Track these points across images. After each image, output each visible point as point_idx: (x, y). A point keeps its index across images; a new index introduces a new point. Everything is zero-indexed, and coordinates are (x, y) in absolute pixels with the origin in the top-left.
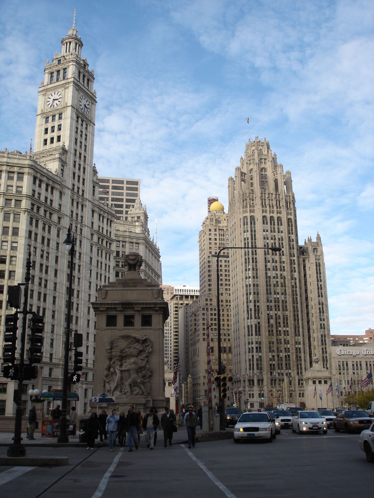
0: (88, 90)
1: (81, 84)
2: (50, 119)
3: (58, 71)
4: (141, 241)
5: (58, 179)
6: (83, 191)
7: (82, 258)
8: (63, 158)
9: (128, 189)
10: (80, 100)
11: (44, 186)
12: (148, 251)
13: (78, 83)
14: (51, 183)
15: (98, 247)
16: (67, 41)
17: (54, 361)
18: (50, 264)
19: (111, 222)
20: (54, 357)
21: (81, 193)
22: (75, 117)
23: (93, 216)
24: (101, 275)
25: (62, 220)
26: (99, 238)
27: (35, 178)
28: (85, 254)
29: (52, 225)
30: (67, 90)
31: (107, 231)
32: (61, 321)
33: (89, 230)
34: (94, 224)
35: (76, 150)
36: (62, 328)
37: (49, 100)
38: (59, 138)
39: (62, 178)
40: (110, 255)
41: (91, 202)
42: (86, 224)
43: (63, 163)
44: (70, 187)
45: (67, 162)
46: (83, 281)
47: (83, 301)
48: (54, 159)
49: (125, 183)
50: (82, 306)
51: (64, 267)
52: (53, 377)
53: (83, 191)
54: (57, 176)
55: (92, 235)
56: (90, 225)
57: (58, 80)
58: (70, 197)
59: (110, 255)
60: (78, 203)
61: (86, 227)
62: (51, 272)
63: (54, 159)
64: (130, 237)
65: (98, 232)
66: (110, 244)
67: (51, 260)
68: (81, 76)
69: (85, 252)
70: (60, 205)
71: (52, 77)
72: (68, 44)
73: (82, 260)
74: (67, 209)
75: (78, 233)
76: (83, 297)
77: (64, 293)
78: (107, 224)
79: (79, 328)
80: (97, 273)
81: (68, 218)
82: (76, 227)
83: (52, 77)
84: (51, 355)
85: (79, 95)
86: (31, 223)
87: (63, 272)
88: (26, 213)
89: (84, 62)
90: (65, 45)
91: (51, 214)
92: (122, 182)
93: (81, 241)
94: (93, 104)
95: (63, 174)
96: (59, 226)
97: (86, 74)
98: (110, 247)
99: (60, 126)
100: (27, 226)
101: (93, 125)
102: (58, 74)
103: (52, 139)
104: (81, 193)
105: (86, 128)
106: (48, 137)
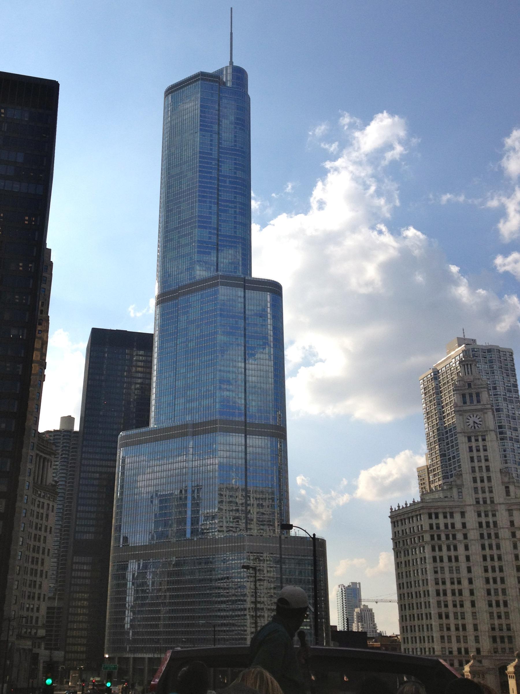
8: (459, 482)
10: (468, 421)
11: (441, 516)
14: (448, 510)
17: (482, 654)
20: (481, 650)
23: (511, 515)
25: (468, 535)
33: (507, 530)
41: (503, 504)
45: (464, 483)
58: (473, 511)
85: (465, 418)
94: (486, 413)
96: (466, 541)
105: (484, 440)
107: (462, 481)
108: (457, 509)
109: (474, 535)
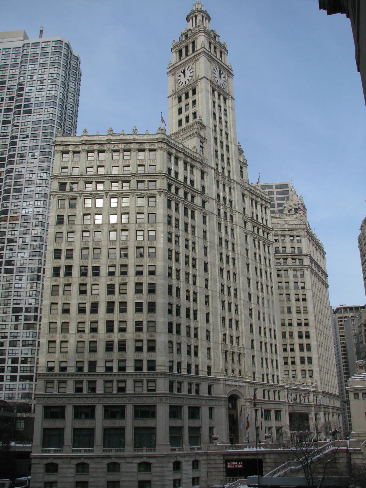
0: (221, 61)
1: (214, 55)
2: (183, 97)
3: (187, 47)
4: (302, 233)
5: (198, 156)
6: (229, 172)
7: (236, 249)
8: (202, 133)
9: (278, 193)
10: (214, 71)
11: (181, 163)
12: (311, 245)
13: (210, 54)
14: (189, 160)
15: (254, 237)
16: (192, 15)
17: (213, 376)
18: (197, 257)
19: (266, 208)
20: (212, 370)
21: (226, 174)
22: (210, 90)
23: (244, 201)
24: (261, 270)
25: (207, 204)
26: (254, 227)
27: (170, 154)
28: (239, 245)
29: (195, 210)
30: (197, 63)
31: (262, 219)
32: (218, 326)
33: (241, 216)
34: (246, 210)
35: (215, 126)
36: (220, 334)
37: (179, 78)
38: (195, 114)
39: (202, 155)
40: (268, 247)
41: (240, 184)
42: (237, 209)
43: (203, 140)
44: (213, 165)
46: (241, 278)
47: (242, 302)
48: (191, 135)
49: (274, 187)
50: (242, 307)
51: (215, 260)
52: (213, 395)
53: (229, 172)
54: (196, 153)
55: (245, 223)
56: (242, 211)
57: (187, 55)
59: (268, 247)
60: (224, 185)
61: (237, 214)
62: (200, 266)
63: (191, 135)
64: (289, 230)
65: (252, 219)
66: (268, 234)
67: (199, 251)
68: (212, 47)
69: (239, 242)
70: (203, 187)
71: (180, 55)
72: (194, 18)
73: (236, 251)
74: (211, 190)
75: (228, 220)
76: (242, 296)
77: (218, 291)
78: (262, 211)
79: (241, 334)
80: (256, 268)
81: (215, 202)
82: (225, 213)
83: (180, 55)
84: (209, 368)
85: (213, 67)
86: (169, 206)
87: (215, 267)
88: (163, 195)
89: (214, 33)
90: (191, 20)
91: (193, 197)
92: (271, 187)
93: (232, 230)
94: (229, 76)
95: (203, 152)
96: (204, 211)
97: (218, 45)
98: (268, 237)
99: (194, 102)
100: (164, 210)
101: (232, 99)
102: (187, 51)
103: (187, 118)
104: (226, 174)
106: (183, 117)
107: (205, 134)
108: (198, 165)
109: (212, 206)
